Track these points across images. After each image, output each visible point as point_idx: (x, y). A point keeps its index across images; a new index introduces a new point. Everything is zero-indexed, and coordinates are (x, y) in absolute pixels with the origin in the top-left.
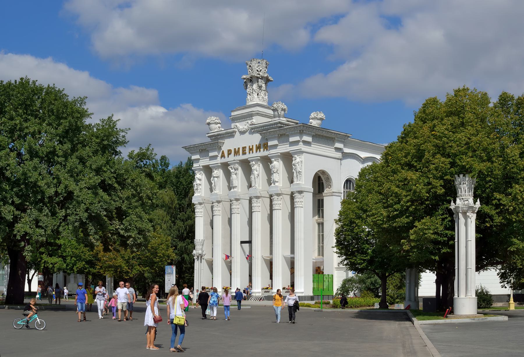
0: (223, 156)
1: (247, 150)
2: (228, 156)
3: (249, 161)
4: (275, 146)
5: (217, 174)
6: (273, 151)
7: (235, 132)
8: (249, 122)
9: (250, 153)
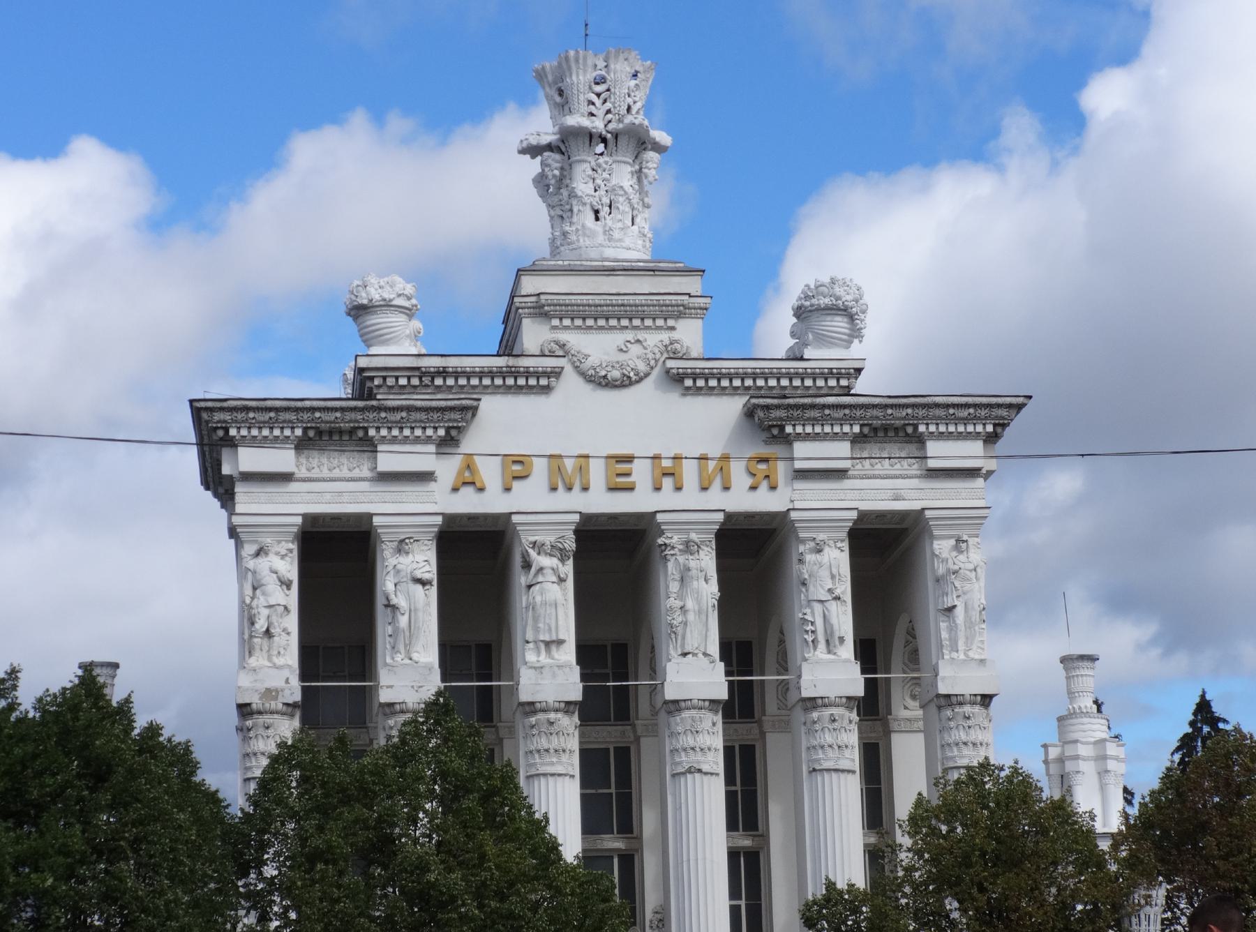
0: (469, 480)
1: (641, 473)
2: (508, 489)
3: (659, 524)
5: (427, 568)
7: (556, 373)
8: (654, 339)
9: (658, 489)
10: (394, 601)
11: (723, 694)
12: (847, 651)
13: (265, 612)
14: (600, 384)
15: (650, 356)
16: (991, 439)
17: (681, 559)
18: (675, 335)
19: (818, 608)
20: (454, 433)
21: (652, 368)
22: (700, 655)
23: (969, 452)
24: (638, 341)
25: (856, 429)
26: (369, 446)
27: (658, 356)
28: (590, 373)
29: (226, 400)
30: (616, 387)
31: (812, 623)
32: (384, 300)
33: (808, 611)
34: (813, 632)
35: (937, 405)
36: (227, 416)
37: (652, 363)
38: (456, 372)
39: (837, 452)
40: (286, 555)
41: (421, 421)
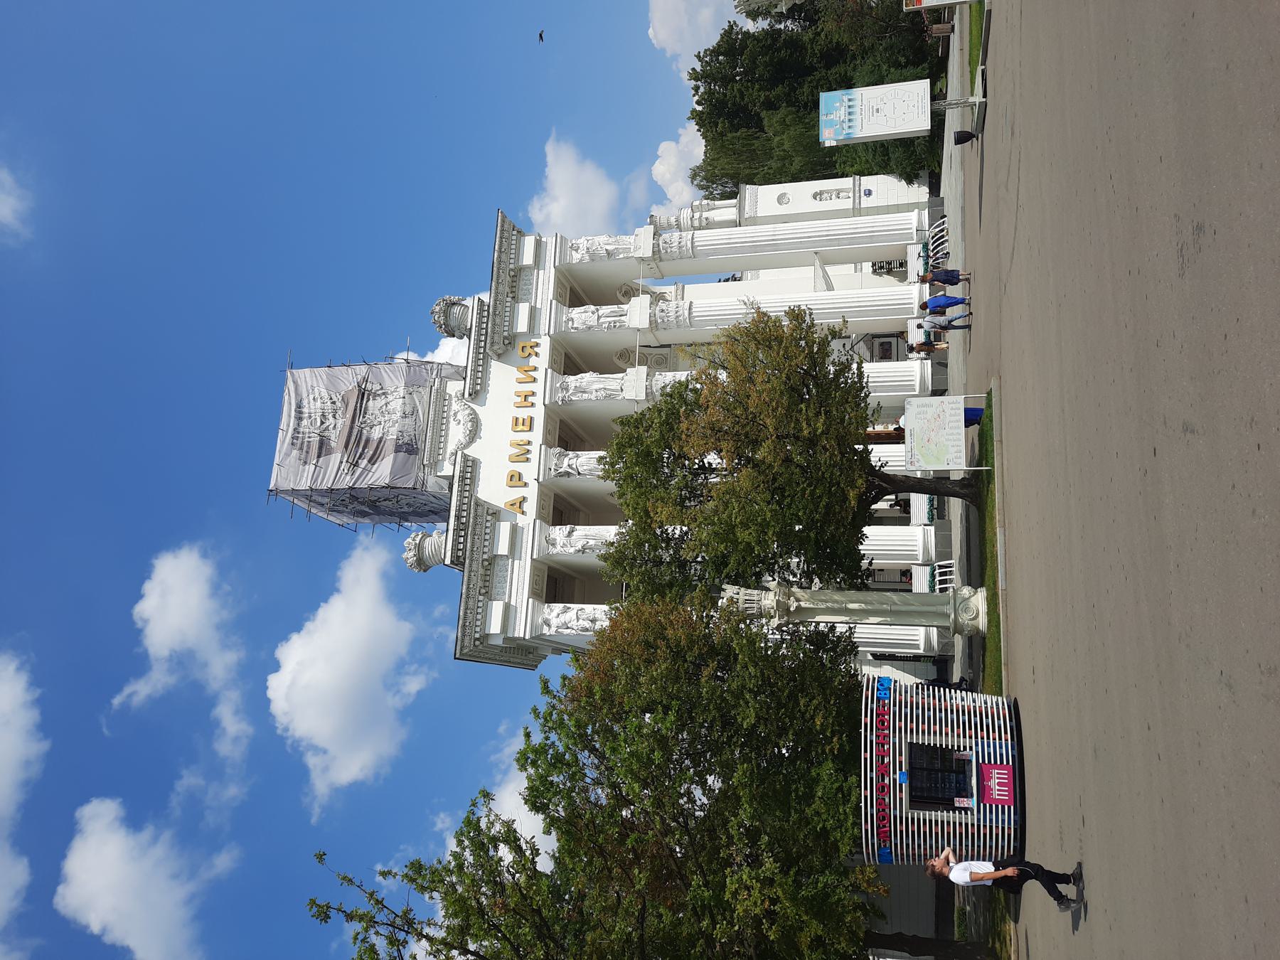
1: (524, 413)
2: (526, 485)
4: (533, 314)
6: (544, 325)
7: (465, 457)
8: (455, 406)
9: (533, 405)
10: (579, 546)
11: (644, 369)
12: (625, 307)
13: (581, 621)
14: (475, 435)
15: (462, 407)
16: (521, 234)
17: (571, 392)
18: (453, 395)
19: (602, 320)
20: (491, 511)
21: (469, 407)
22: (623, 382)
23: (529, 242)
24: (455, 414)
25: (509, 299)
26: (493, 560)
27: (463, 404)
28: (467, 439)
29: (457, 637)
30: (477, 426)
31: (610, 323)
32: (415, 548)
33: (604, 325)
34: (615, 323)
35: (499, 257)
36: (467, 639)
37: (466, 406)
38: (459, 509)
39: (523, 309)
40: (551, 609)
41: (481, 528)
